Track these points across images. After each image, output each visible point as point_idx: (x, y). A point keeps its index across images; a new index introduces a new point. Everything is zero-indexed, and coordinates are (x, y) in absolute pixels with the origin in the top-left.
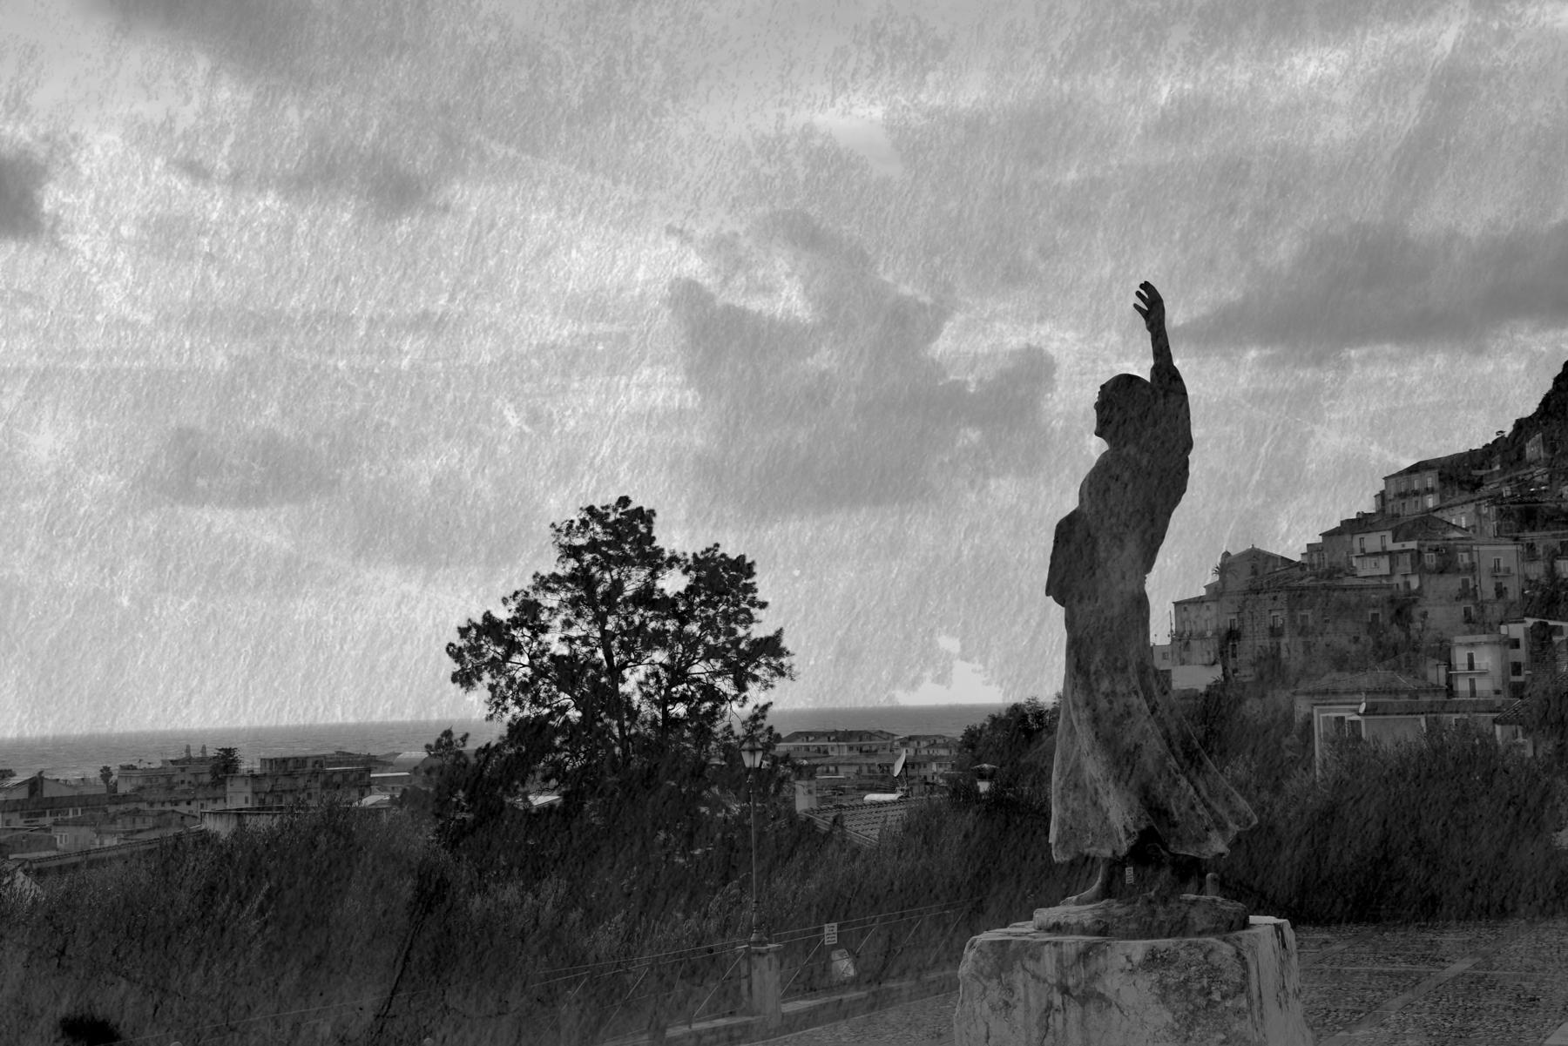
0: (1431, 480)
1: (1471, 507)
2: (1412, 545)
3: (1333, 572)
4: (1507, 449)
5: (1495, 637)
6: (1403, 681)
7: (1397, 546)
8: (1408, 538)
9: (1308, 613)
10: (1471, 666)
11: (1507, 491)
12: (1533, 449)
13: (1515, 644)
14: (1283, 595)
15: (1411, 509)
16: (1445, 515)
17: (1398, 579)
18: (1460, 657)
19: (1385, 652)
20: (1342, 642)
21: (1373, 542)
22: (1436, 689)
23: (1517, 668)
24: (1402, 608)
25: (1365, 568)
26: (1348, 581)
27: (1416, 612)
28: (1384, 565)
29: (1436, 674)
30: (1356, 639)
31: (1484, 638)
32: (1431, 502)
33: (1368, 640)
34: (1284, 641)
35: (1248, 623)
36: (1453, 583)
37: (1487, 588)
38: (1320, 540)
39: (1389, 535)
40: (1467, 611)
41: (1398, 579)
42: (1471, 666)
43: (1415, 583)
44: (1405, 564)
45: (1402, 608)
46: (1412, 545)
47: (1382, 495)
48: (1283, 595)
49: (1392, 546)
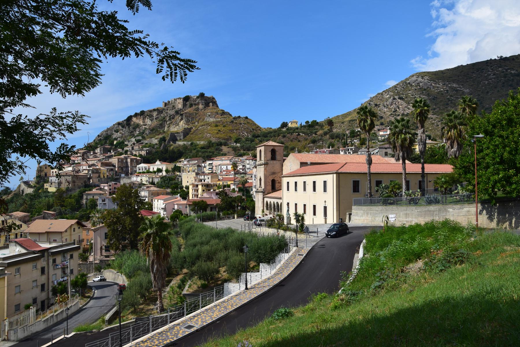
13: (110, 186)
20: (80, 184)
36: (97, 175)
37: (102, 176)
49: (88, 168)
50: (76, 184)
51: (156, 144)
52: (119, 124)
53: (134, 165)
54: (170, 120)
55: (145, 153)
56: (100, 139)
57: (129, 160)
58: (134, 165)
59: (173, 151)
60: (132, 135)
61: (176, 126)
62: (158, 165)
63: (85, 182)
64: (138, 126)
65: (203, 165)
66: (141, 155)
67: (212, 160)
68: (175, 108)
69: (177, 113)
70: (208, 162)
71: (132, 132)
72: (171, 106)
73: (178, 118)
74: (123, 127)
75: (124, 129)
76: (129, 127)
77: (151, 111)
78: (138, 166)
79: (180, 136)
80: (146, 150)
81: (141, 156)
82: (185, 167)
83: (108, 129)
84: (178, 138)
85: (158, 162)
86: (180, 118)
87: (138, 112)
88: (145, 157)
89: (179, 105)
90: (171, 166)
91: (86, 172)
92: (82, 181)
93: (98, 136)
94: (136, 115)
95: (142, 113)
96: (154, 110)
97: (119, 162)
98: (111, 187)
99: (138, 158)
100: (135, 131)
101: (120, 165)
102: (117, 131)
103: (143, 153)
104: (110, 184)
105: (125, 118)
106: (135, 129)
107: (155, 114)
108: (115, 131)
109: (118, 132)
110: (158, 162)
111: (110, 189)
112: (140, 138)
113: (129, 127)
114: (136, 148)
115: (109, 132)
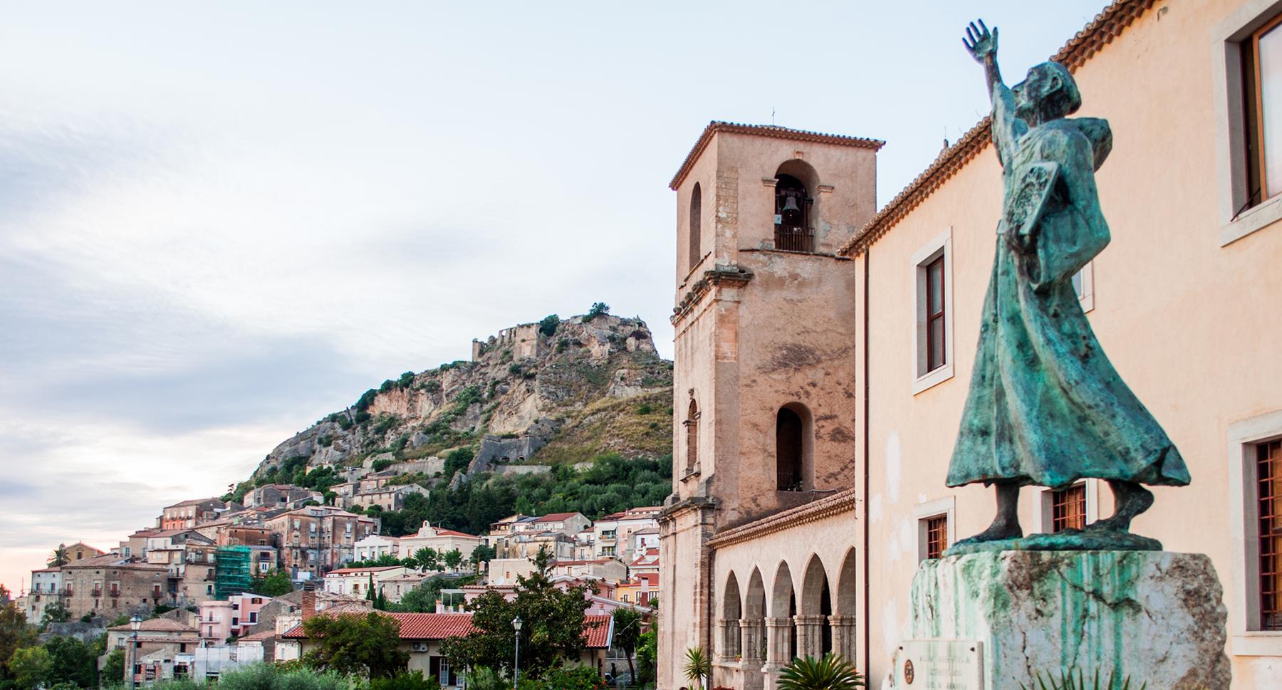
0: (191, 512)
1: (215, 529)
2: (182, 547)
3: (133, 559)
4: (236, 498)
5: (226, 603)
6: (175, 625)
7: (174, 547)
8: (181, 542)
9: (118, 583)
10: (211, 619)
11: (235, 521)
12: (249, 500)
13: (236, 607)
14: (103, 572)
15: (178, 528)
16: (199, 531)
17: (172, 567)
18: (205, 613)
19: (160, 610)
20: (137, 602)
21: (160, 543)
22: (192, 631)
23: (235, 621)
24: (173, 583)
25: (154, 558)
26: (144, 566)
27: (180, 587)
28: (164, 558)
29: (193, 621)
30: (145, 601)
31: (220, 603)
32: (190, 524)
33: (151, 601)
34: (101, 599)
35: (79, 586)
38: (128, 539)
39: (170, 540)
40: (210, 587)
41: (172, 567)
42: (211, 619)
43: (182, 569)
44: (177, 556)
45: (173, 583)
46: (182, 547)
47: (161, 518)
48: (103, 572)
50: (122, 600)
51: (438, 475)
52: (334, 418)
53: (344, 542)
54: (492, 396)
55: (392, 502)
56: (274, 470)
57: (328, 524)
58: (344, 542)
59: (488, 497)
60: (370, 447)
61: (510, 414)
62: (429, 537)
63: (156, 596)
64: (392, 422)
65: (583, 537)
66: (379, 508)
67: (617, 519)
68: (511, 358)
69: (515, 371)
70: (601, 526)
71: (373, 443)
72: (500, 353)
73: (518, 387)
74: (347, 426)
75: (350, 437)
76: (365, 428)
77: (434, 374)
78: (357, 544)
79: (520, 448)
80: (399, 492)
81: (376, 511)
82: (511, 542)
83: (300, 437)
84: (513, 455)
85: (426, 530)
86: (523, 388)
87: (396, 377)
88: (390, 515)
89: (527, 351)
90: (467, 545)
91: (164, 558)
92: (146, 592)
93: (268, 457)
94: (388, 387)
95: (408, 380)
96: (445, 368)
97: (293, 528)
98: (237, 614)
99: (364, 518)
100: (383, 439)
101: (296, 541)
102: (326, 442)
103: (387, 501)
104: (236, 599)
105: (355, 399)
106: (381, 431)
107: (446, 381)
108: (320, 442)
109: (329, 444)
110: (426, 530)
111: (235, 621)
112: (389, 457)
113: (365, 428)
114: (368, 486)
115: (302, 447)
